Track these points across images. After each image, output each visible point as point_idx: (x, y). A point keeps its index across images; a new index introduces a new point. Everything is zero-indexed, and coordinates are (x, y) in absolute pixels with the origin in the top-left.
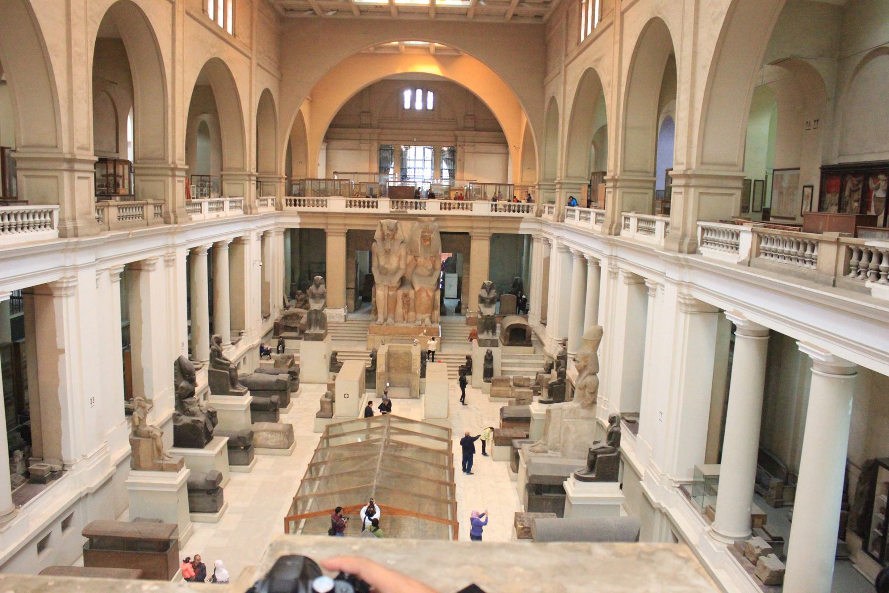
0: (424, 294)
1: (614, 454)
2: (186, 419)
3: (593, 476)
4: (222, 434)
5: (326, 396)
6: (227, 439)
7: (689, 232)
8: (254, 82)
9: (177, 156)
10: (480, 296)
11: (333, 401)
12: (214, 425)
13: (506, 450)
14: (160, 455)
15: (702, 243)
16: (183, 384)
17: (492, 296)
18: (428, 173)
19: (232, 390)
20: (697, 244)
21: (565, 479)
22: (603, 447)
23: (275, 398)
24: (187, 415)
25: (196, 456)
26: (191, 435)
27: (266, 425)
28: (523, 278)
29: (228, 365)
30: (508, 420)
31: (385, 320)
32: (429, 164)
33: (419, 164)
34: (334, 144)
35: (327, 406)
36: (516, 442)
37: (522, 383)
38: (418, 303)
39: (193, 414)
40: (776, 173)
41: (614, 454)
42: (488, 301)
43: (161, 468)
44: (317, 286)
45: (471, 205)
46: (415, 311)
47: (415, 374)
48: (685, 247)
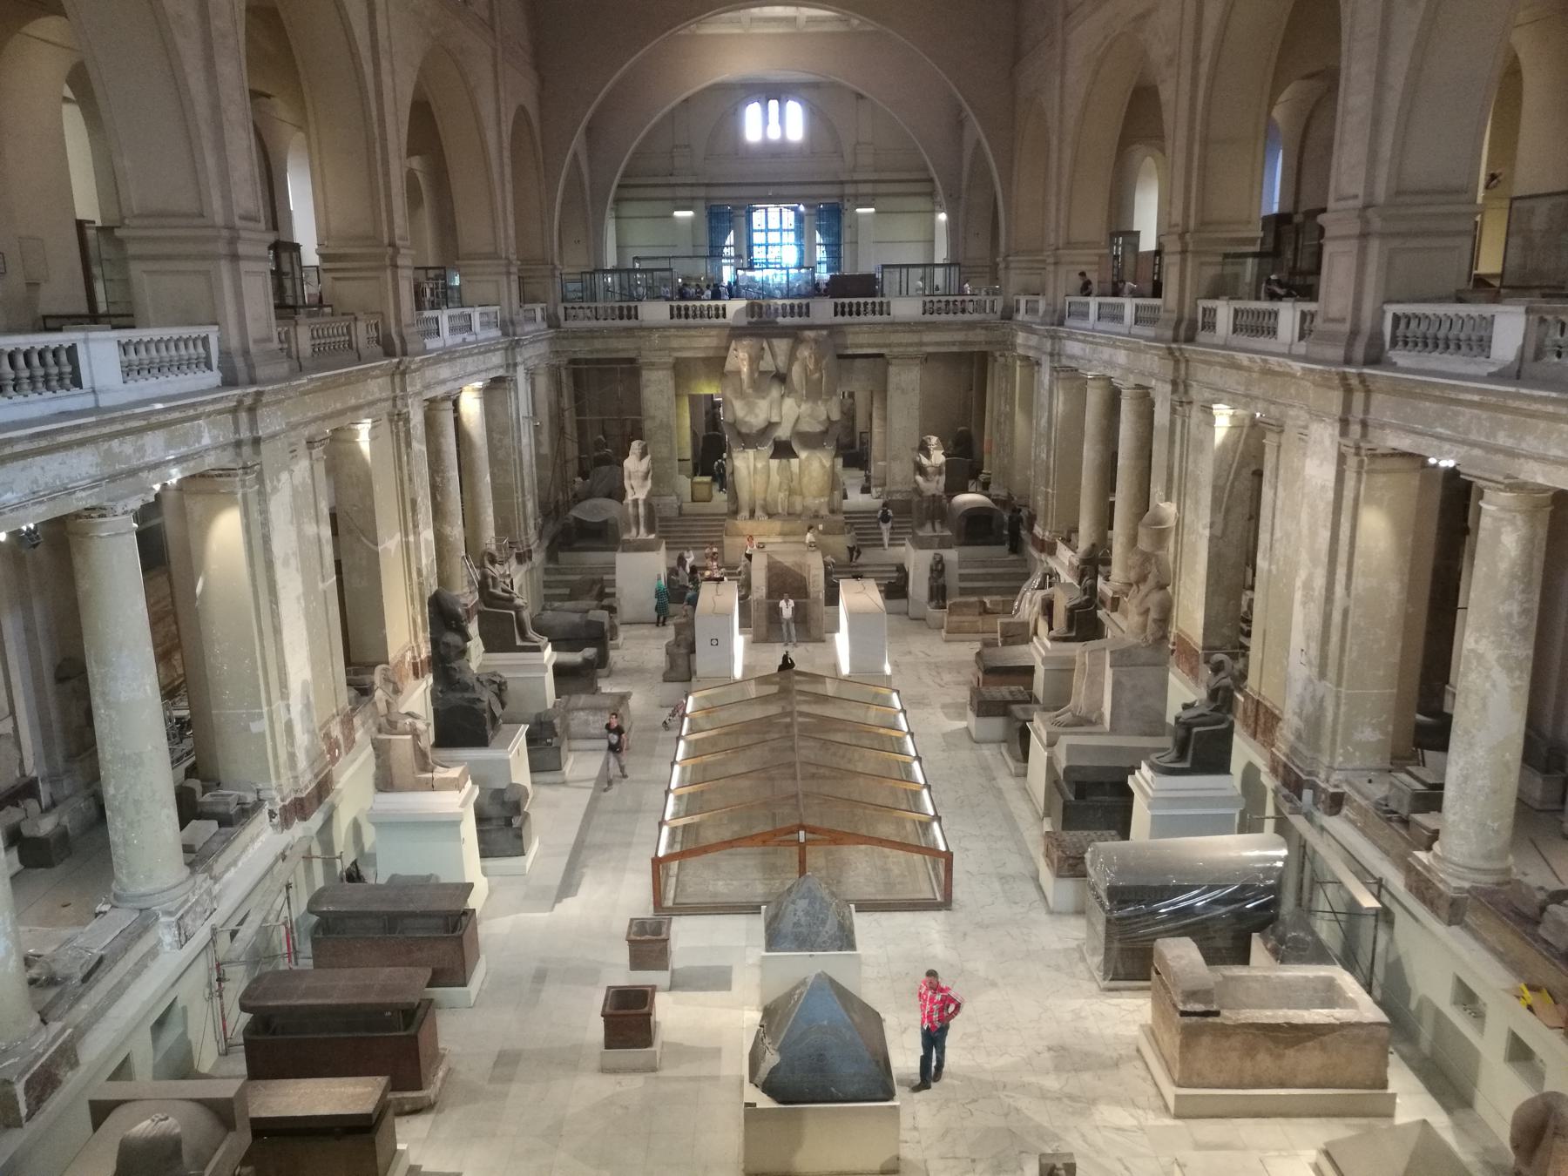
1: (1223, 726)
2: (456, 697)
3: (1187, 765)
4: (514, 721)
5: (677, 643)
6: (524, 729)
7: (1366, 325)
8: (502, 94)
9: (398, 232)
11: (692, 650)
12: (503, 705)
13: (996, 725)
14: (426, 763)
15: (1394, 343)
18: (790, 256)
19: (519, 643)
20: (1383, 345)
21: (1132, 770)
22: (1203, 715)
23: (590, 652)
26: (462, 723)
27: (583, 699)
28: (973, 431)
30: (994, 672)
34: (629, 209)
35: (681, 662)
36: (1015, 708)
38: (805, 480)
40: (1516, 204)
41: (1223, 726)
47: (817, 600)
48: (1359, 352)
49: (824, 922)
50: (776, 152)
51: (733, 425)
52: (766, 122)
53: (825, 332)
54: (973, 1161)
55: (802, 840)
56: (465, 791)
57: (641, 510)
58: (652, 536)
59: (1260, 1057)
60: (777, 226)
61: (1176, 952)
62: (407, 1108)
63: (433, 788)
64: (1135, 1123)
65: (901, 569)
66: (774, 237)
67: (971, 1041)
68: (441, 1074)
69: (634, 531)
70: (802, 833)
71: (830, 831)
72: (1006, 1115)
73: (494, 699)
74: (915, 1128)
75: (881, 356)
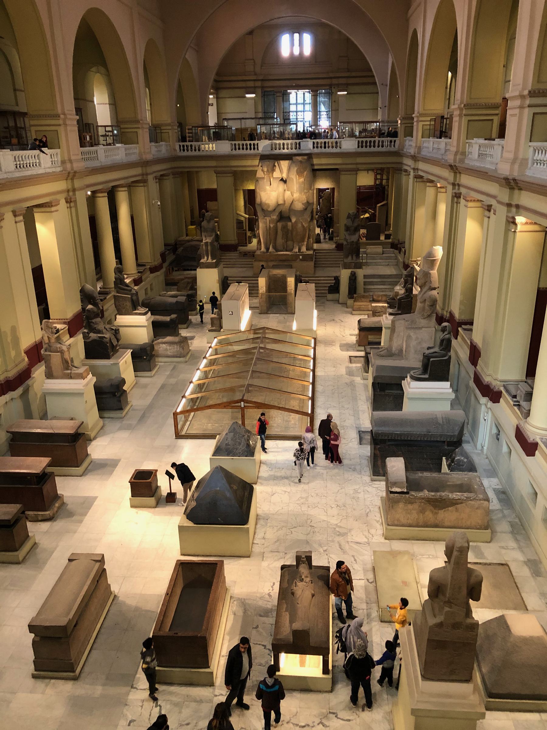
0: (300, 225)
3: (427, 376)
6: (129, 352)
10: (345, 225)
12: (118, 340)
16: (90, 307)
17: (356, 224)
18: (309, 116)
21: (404, 378)
22: (436, 352)
24: (94, 333)
25: (105, 366)
29: (131, 291)
31: (268, 249)
32: (308, 107)
33: (300, 107)
34: (223, 93)
37: (380, 298)
38: (294, 233)
39: (99, 332)
42: (353, 228)
43: (70, 377)
44: (209, 221)
45: (340, 142)
46: (293, 240)
47: (291, 294)
49: (240, 444)
50: (297, 61)
51: (261, 204)
52: (292, 44)
53: (306, 157)
54: (286, 553)
55: (243, 406)
56: (86, 380)
57: (209, 248)
58: (214, 261)
59: (427, 513)
60: (295, 102)
61: (393, 464)
62: (40, 518)
63: (71, 378)
64: (366, 540)
65: (337, 279)
66: (300, 107)
67: (302, 500)
68: (57, 505)
69: (206, 258)
70: (242, 403)
71: (255, 402)
72: (307, 534)
73: (113, 337)
74: (264, 538)
75: (337, 169)
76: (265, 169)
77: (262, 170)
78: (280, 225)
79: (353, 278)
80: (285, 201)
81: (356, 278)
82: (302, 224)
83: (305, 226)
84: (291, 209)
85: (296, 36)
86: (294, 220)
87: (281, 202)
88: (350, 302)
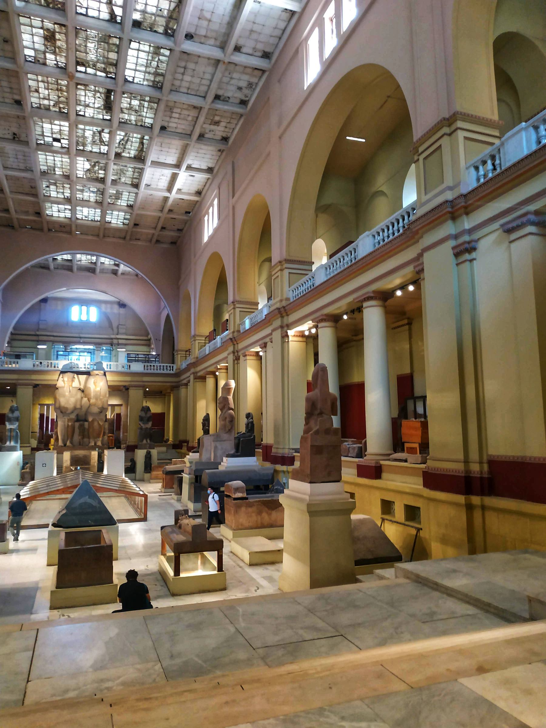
0: (96, 424)
38: (91, 430)
50: (84, 326)
76: (66, 379)
77: (63, 381)
78: (77, 424)
79: (149, 456)
80: (81, 407)
81: (151, 455)
82: (98, 423)
83: (101, 424)
84: (87, 413)
85: (84, 308)
86: (90, 419)
87: (78, 406)
88: (147, 475)
